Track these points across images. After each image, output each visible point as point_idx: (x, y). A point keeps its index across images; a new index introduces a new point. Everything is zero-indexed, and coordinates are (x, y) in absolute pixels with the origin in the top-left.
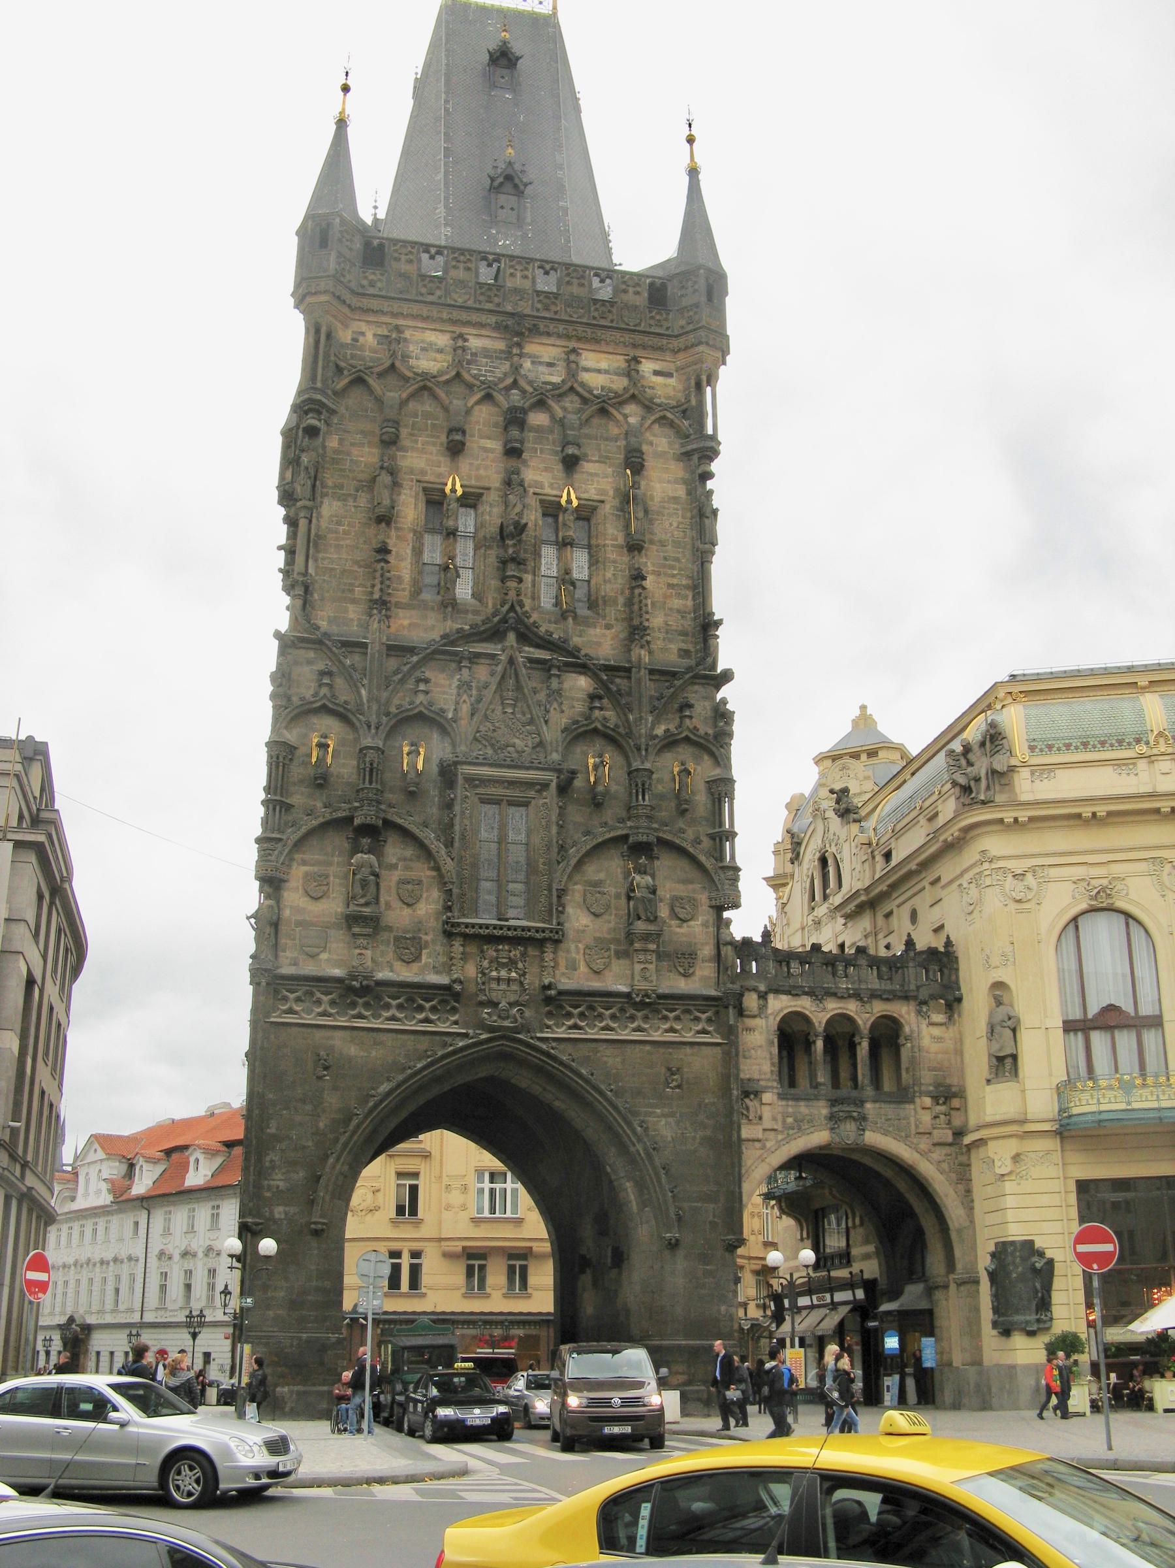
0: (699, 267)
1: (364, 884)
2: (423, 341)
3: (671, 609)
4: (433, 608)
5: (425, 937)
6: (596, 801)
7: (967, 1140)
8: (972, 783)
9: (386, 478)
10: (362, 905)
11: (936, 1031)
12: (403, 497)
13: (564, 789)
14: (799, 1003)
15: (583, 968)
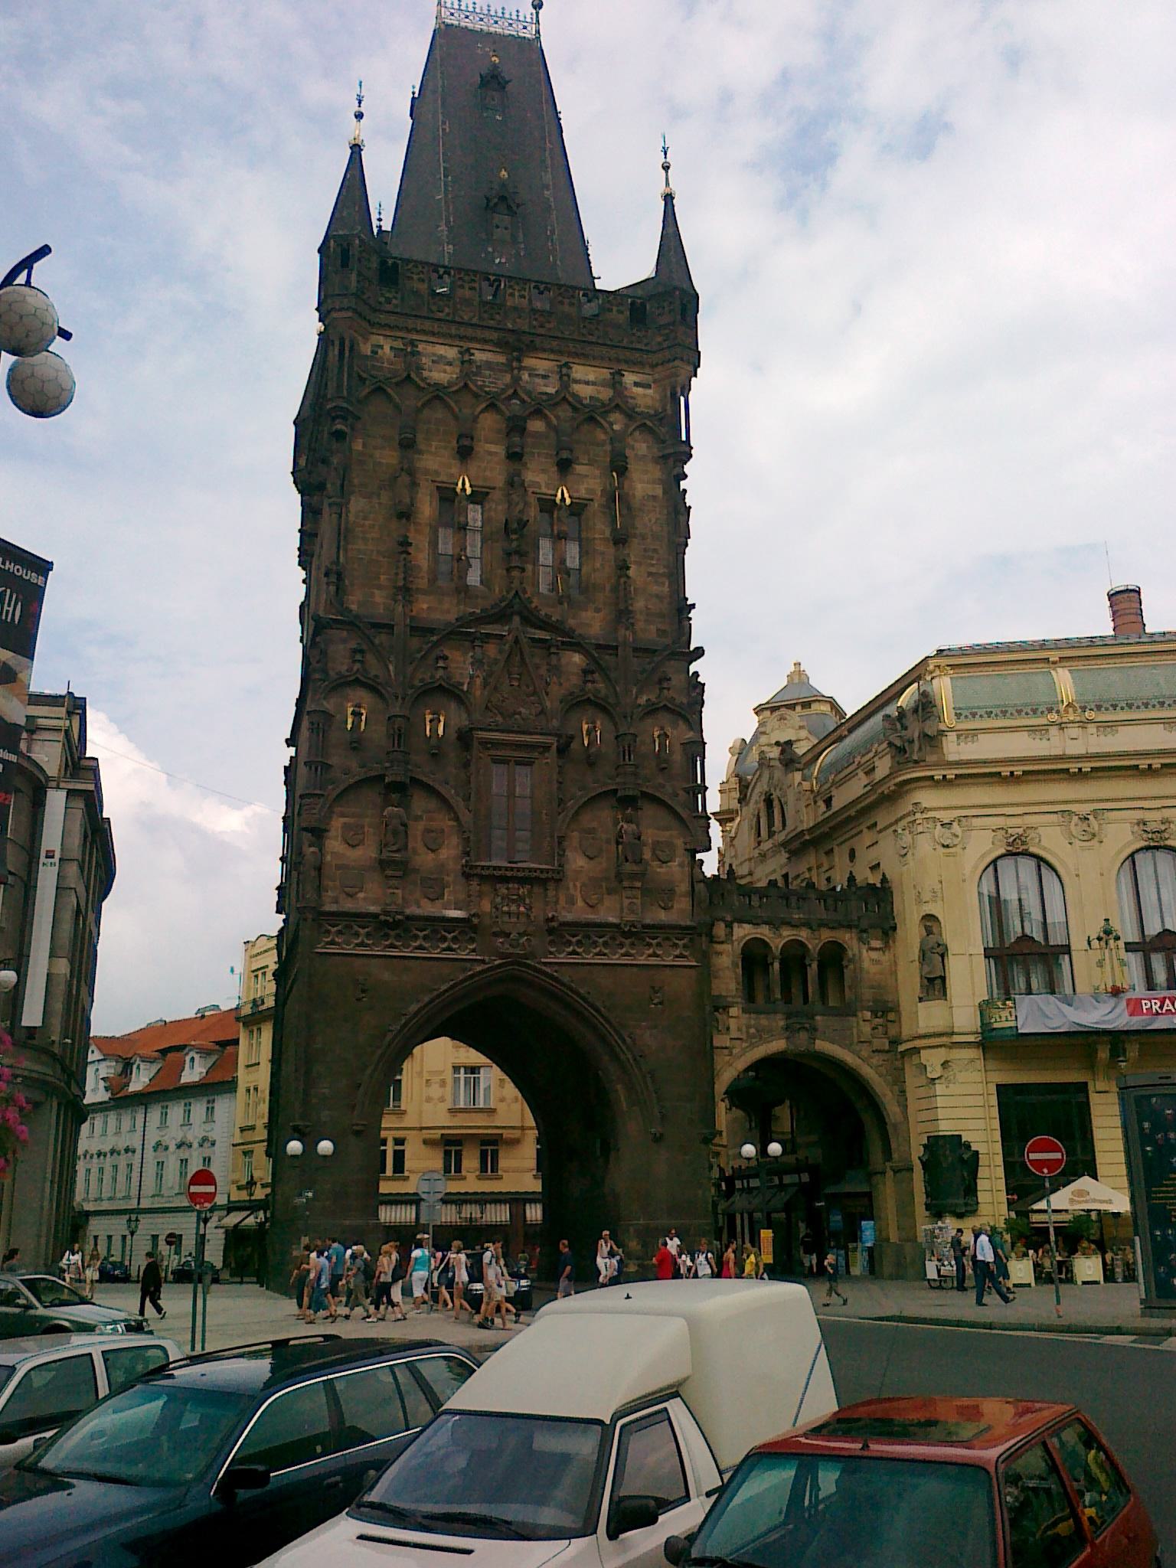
0: (676, 288)
1: (395, 833)
2: (434, 355)
5: (446, 878)
6: (591, 761)
7: (901, 1048)
8: (906, 744)
9: (405, 479)
11: (874, 955)
12: (420, 495)
13: (562, 751)
14: (759, 930)
15: (580, 903)
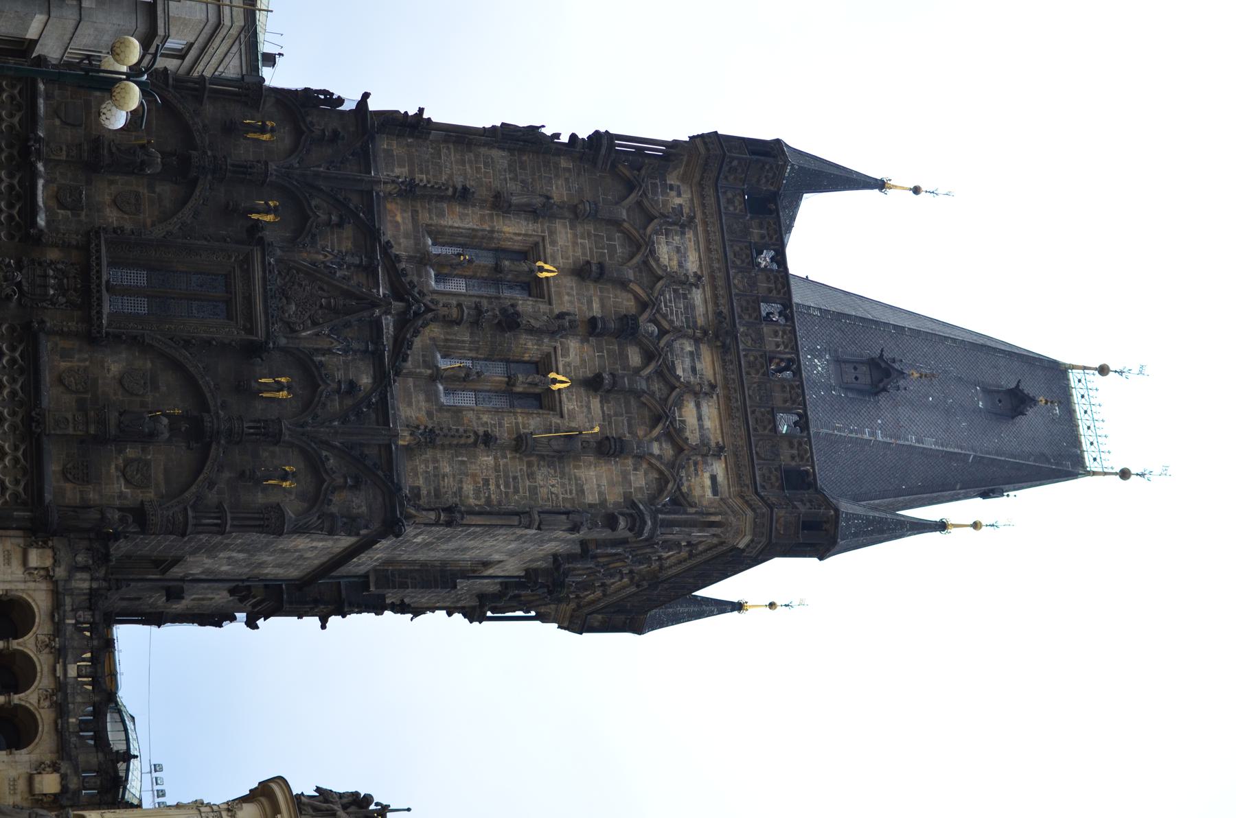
2: (686, 249)
3: (461, 481)
4: (417, 244)
5: (84, 213)
10: (110, 150)
12: (524, 223)
15: (64, 365)
